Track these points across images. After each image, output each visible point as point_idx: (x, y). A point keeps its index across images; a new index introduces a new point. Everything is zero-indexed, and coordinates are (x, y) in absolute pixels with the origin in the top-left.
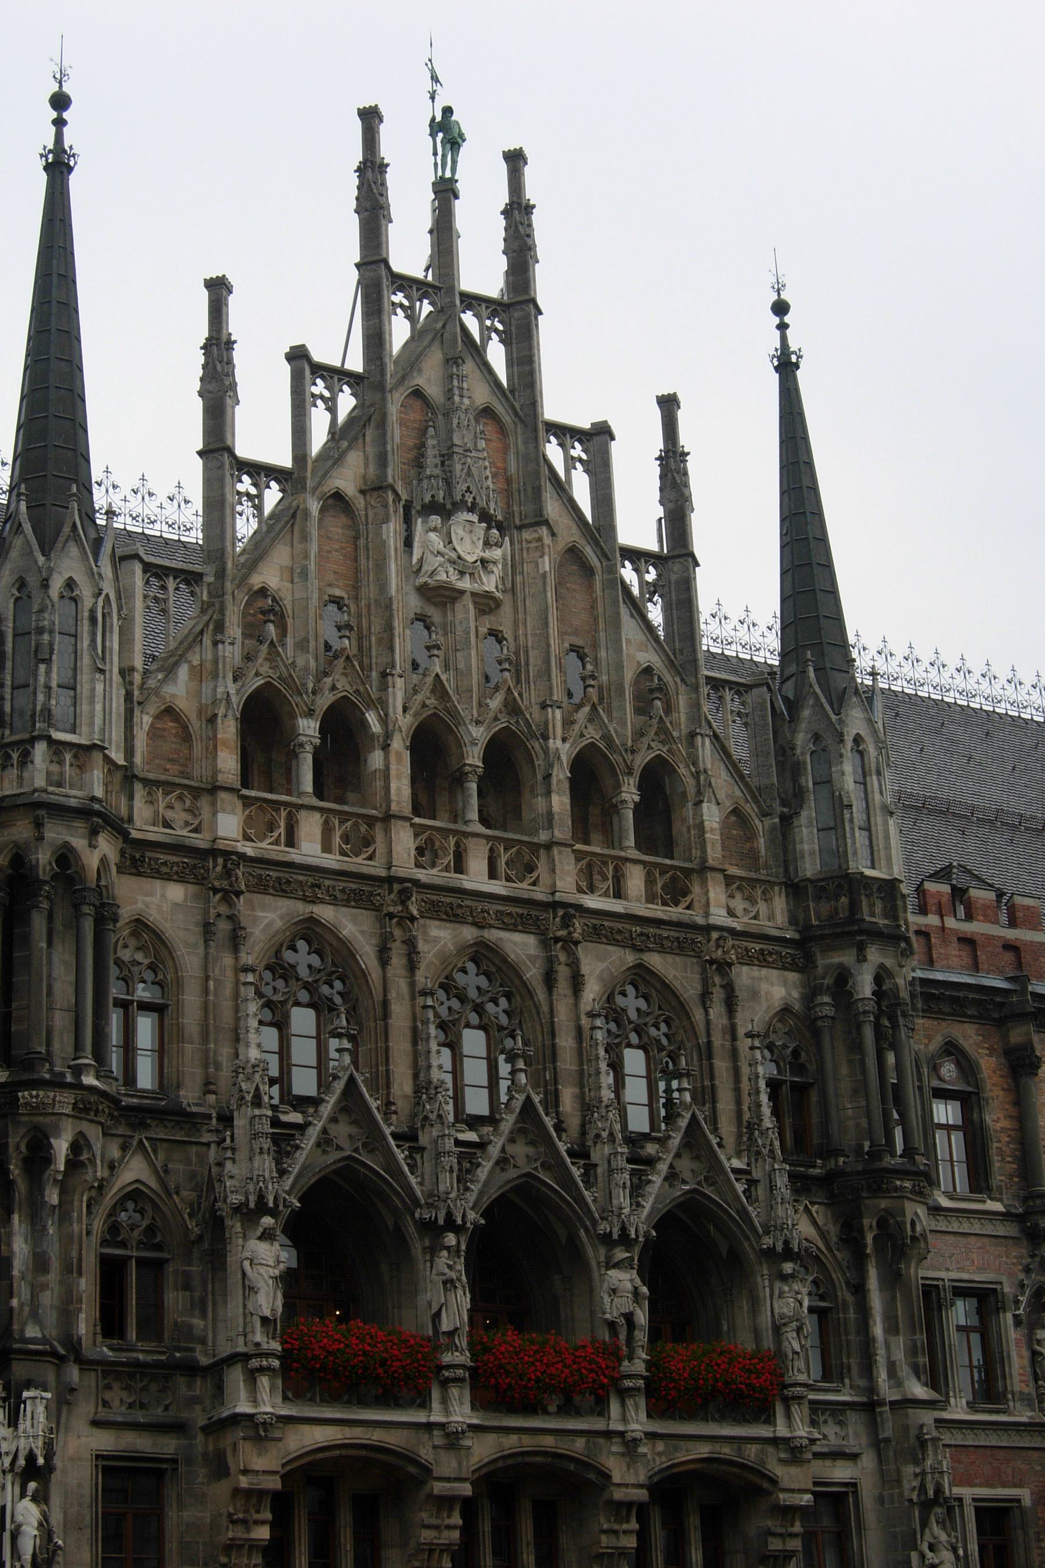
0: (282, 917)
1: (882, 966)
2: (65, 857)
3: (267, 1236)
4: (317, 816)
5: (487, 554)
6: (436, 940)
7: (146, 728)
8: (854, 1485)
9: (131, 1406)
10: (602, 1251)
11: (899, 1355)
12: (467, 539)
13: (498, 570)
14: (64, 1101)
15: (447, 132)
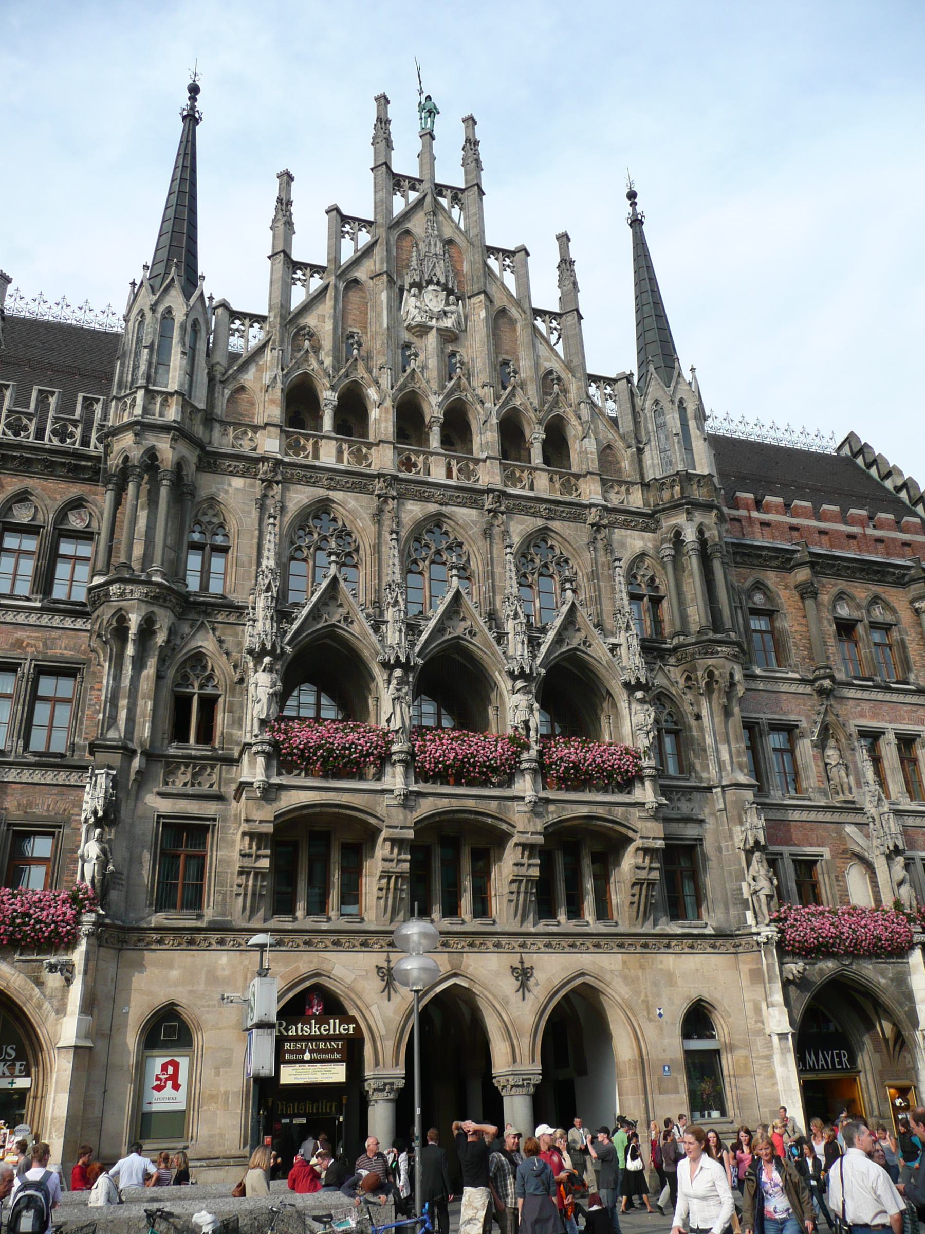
0: (308, 497)
1: (701, 524)
2: (152, 454)
3: (270, 669)
4: (334, 442)
5: (447, 309)
6: (411, 511)
7: (227, 396)
8: (701, 840)
9: (185, 784)
10: (510, 683)
11: (725, 757)
12: (434, 300)
13: (454, 316)
14: (139, 591)
15: (429, 110)
